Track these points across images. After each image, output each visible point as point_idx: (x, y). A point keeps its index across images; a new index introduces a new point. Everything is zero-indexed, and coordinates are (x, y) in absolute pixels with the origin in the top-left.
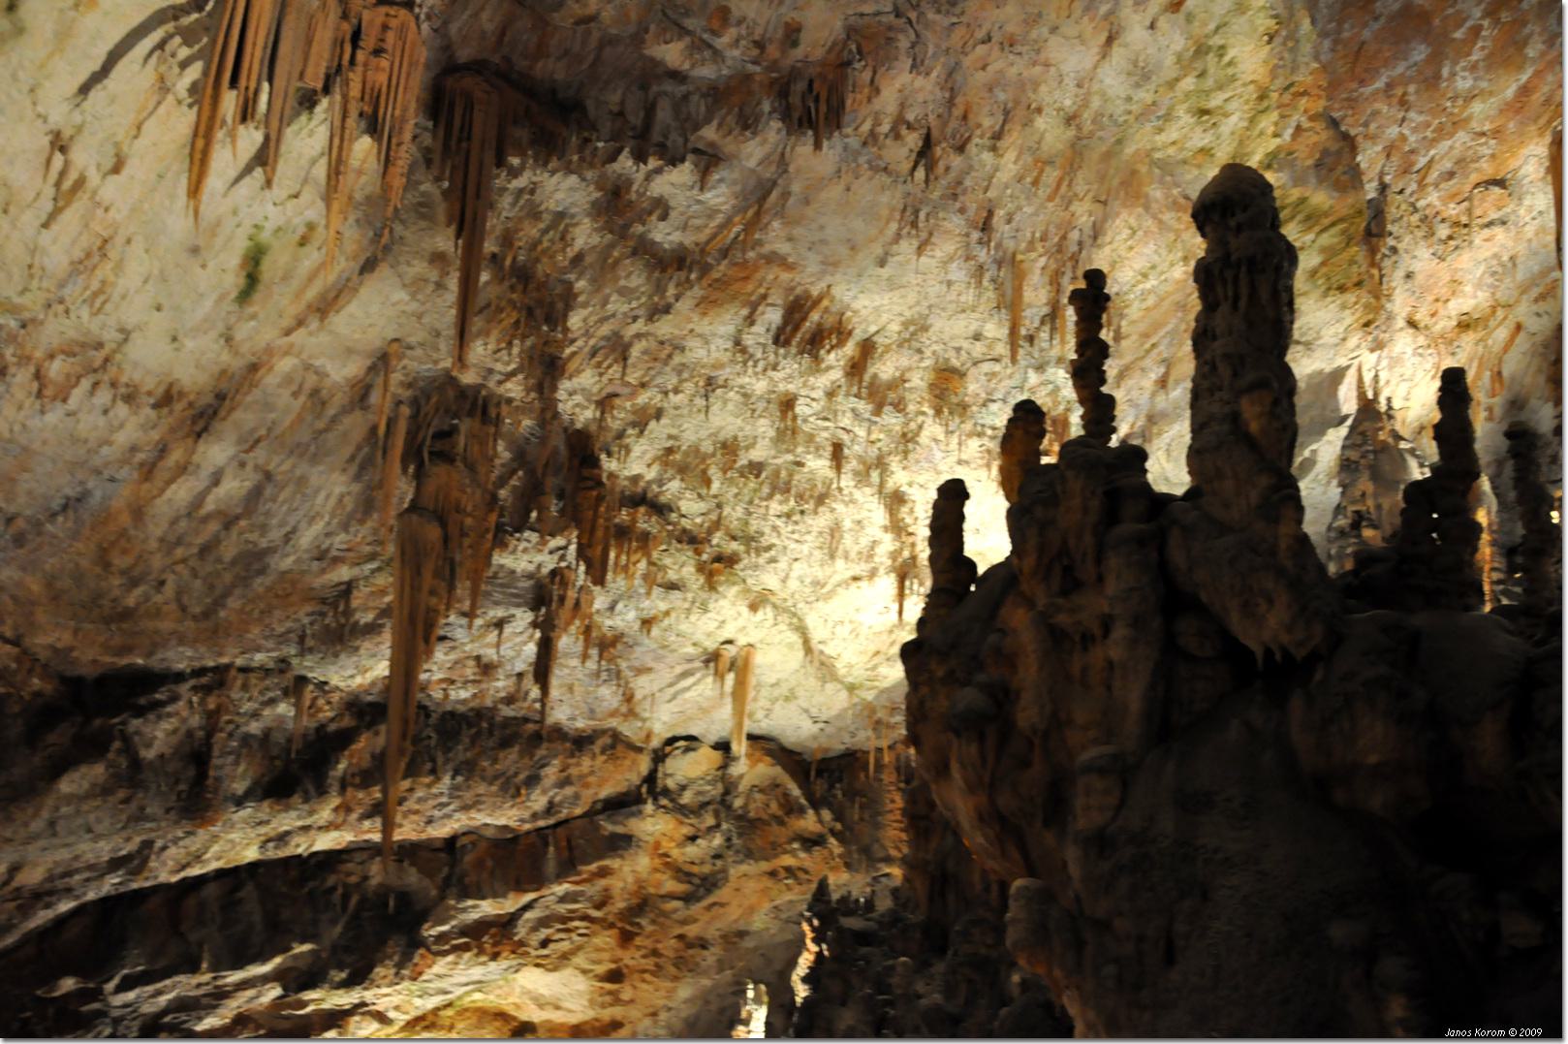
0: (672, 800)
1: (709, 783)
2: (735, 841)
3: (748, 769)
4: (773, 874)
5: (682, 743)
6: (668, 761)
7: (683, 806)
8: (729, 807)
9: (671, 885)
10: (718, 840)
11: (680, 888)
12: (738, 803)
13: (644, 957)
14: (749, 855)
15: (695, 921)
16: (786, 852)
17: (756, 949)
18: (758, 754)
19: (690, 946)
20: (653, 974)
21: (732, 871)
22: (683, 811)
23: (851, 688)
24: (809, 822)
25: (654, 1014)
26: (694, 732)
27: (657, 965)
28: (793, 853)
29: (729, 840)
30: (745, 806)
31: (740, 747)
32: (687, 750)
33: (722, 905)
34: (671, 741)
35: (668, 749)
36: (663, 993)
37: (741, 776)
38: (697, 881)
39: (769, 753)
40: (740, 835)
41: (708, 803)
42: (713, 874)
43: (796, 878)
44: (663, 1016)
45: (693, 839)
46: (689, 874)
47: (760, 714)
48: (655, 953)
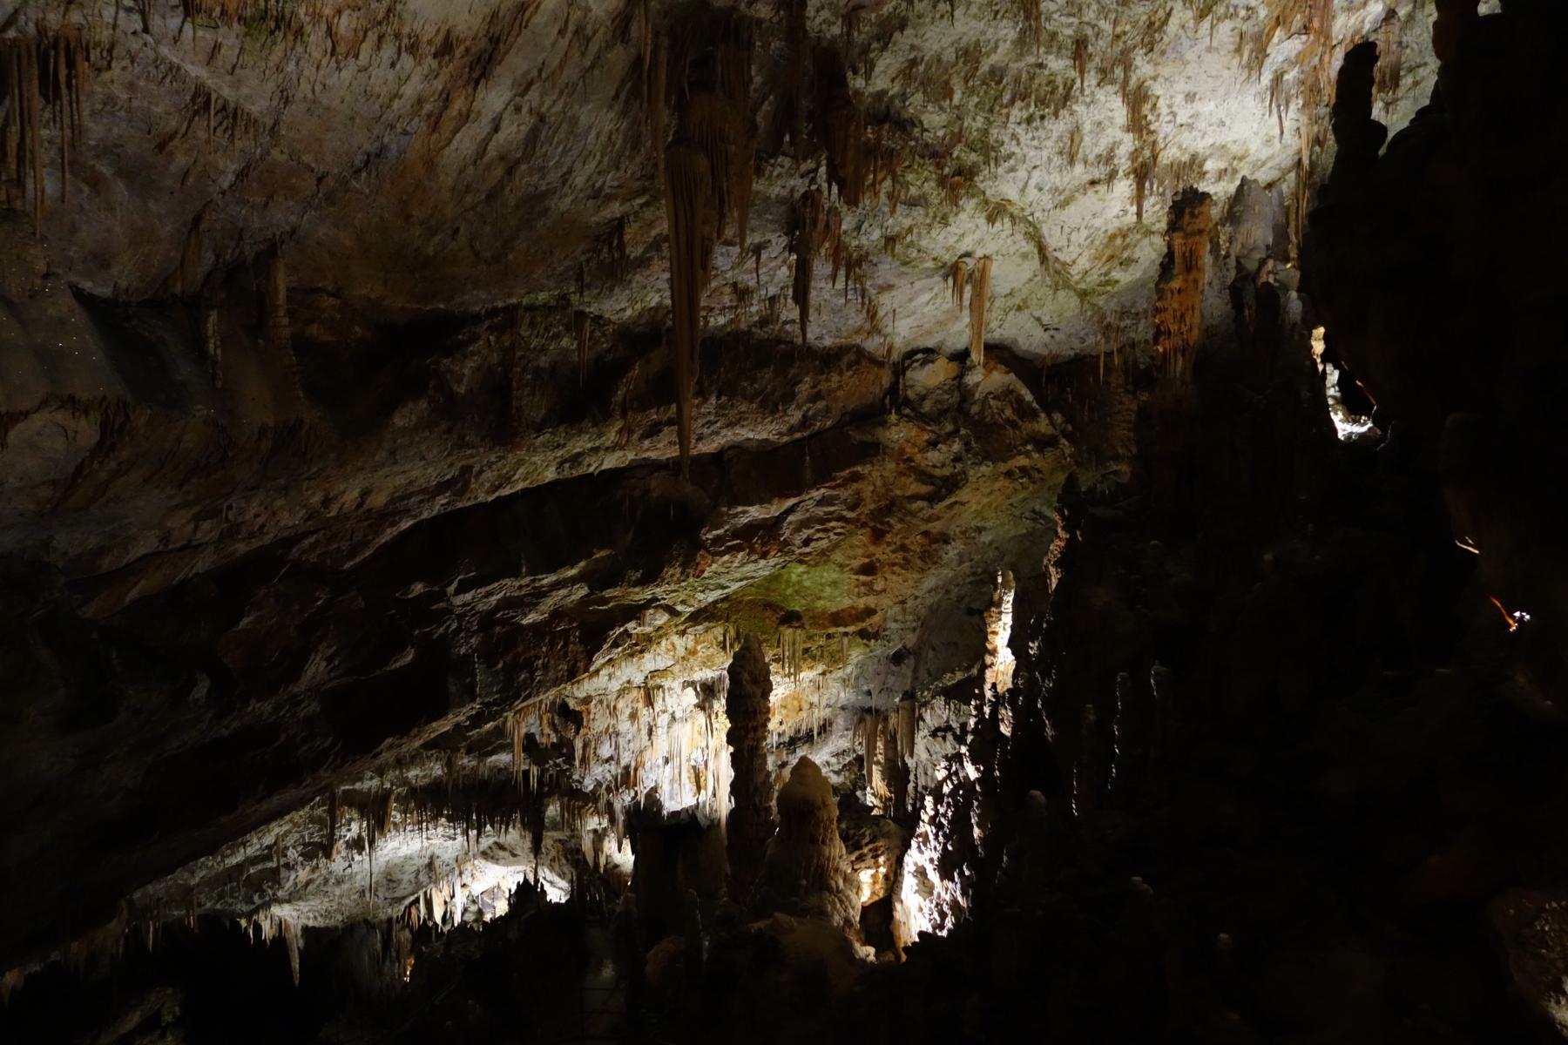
0: (913, 409)
1: (946, 392)
2: (973, 444)
3: (985, 380)
4: (1009, 474)
5: (920, 356)
6: (908, 373)
7: (924, 415)
8: (967, 414)
9: (916, 488)
10: (957, 446)
11: (925, 489)
12: (975, 409)
13: (894, 552)
14: (987, 456)
15: (939, 518)
16: (1020, 453)
17: (991, 543)
18: (992, 364)
19: (934, 541)
20: (902, 567)
21: (972, 472)
22: (923, 419)
23: (1083, 295)
24: (1043, 426)
25: (903, 602)
26: (930, 343)
27: (905, 559)
28: (1027, 454)
29: (967, 444)
30: (982, 411)
31: (977, 356)
32: (925, 363)
33: (962, 504)
34: (913, 352)
35: (907, 363)
36: (911, 583)
37: (977, 385)
38: (938, 482)
39: (1003, 362)
40: (977, 440)
41: (946, 411)
42: (953, 475)
43: (1030, 477)
44: (910, 603)
45: (933, 444)
46: (932, 476)
47: (994, 325)
48: (903, 548)
